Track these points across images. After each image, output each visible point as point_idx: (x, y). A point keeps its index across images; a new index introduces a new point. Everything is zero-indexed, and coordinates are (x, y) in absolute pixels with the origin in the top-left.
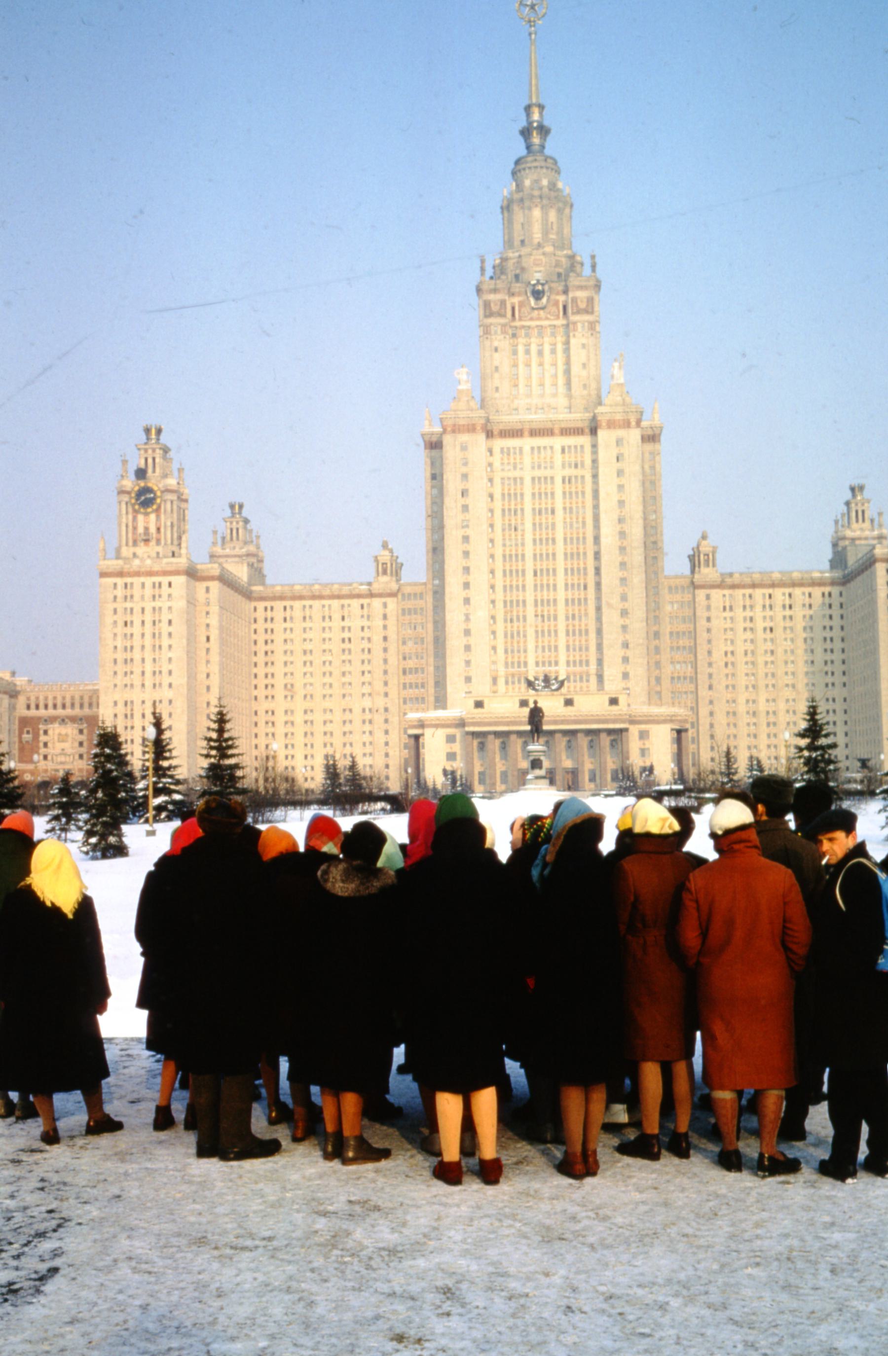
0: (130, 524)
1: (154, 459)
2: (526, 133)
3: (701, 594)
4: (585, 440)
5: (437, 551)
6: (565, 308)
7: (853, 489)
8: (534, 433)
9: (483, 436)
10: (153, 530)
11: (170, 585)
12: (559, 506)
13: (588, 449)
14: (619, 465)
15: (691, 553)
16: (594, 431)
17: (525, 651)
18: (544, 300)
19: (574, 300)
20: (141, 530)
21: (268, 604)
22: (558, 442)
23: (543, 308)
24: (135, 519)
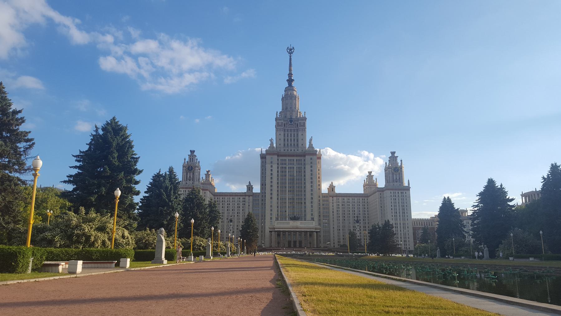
0: (186, 175)
1: (193, 158)
2: (287, 80)
3: (331, 198)
4: (302, 158)
5: (263, 185)
6: (297, 124)
7: (369, 172)
8: (289, 156)
9: (276, 156)
10: (192, 176)
12: (295, 175)
13: (303, 160)
14: (311, 165)
15: (328, 187)
16: (304, 156)
17: (286, 211)
18: (292, 123)
21: (218, 197)
22: (295, 158)
23: (292, 125)
24: (187, 174)
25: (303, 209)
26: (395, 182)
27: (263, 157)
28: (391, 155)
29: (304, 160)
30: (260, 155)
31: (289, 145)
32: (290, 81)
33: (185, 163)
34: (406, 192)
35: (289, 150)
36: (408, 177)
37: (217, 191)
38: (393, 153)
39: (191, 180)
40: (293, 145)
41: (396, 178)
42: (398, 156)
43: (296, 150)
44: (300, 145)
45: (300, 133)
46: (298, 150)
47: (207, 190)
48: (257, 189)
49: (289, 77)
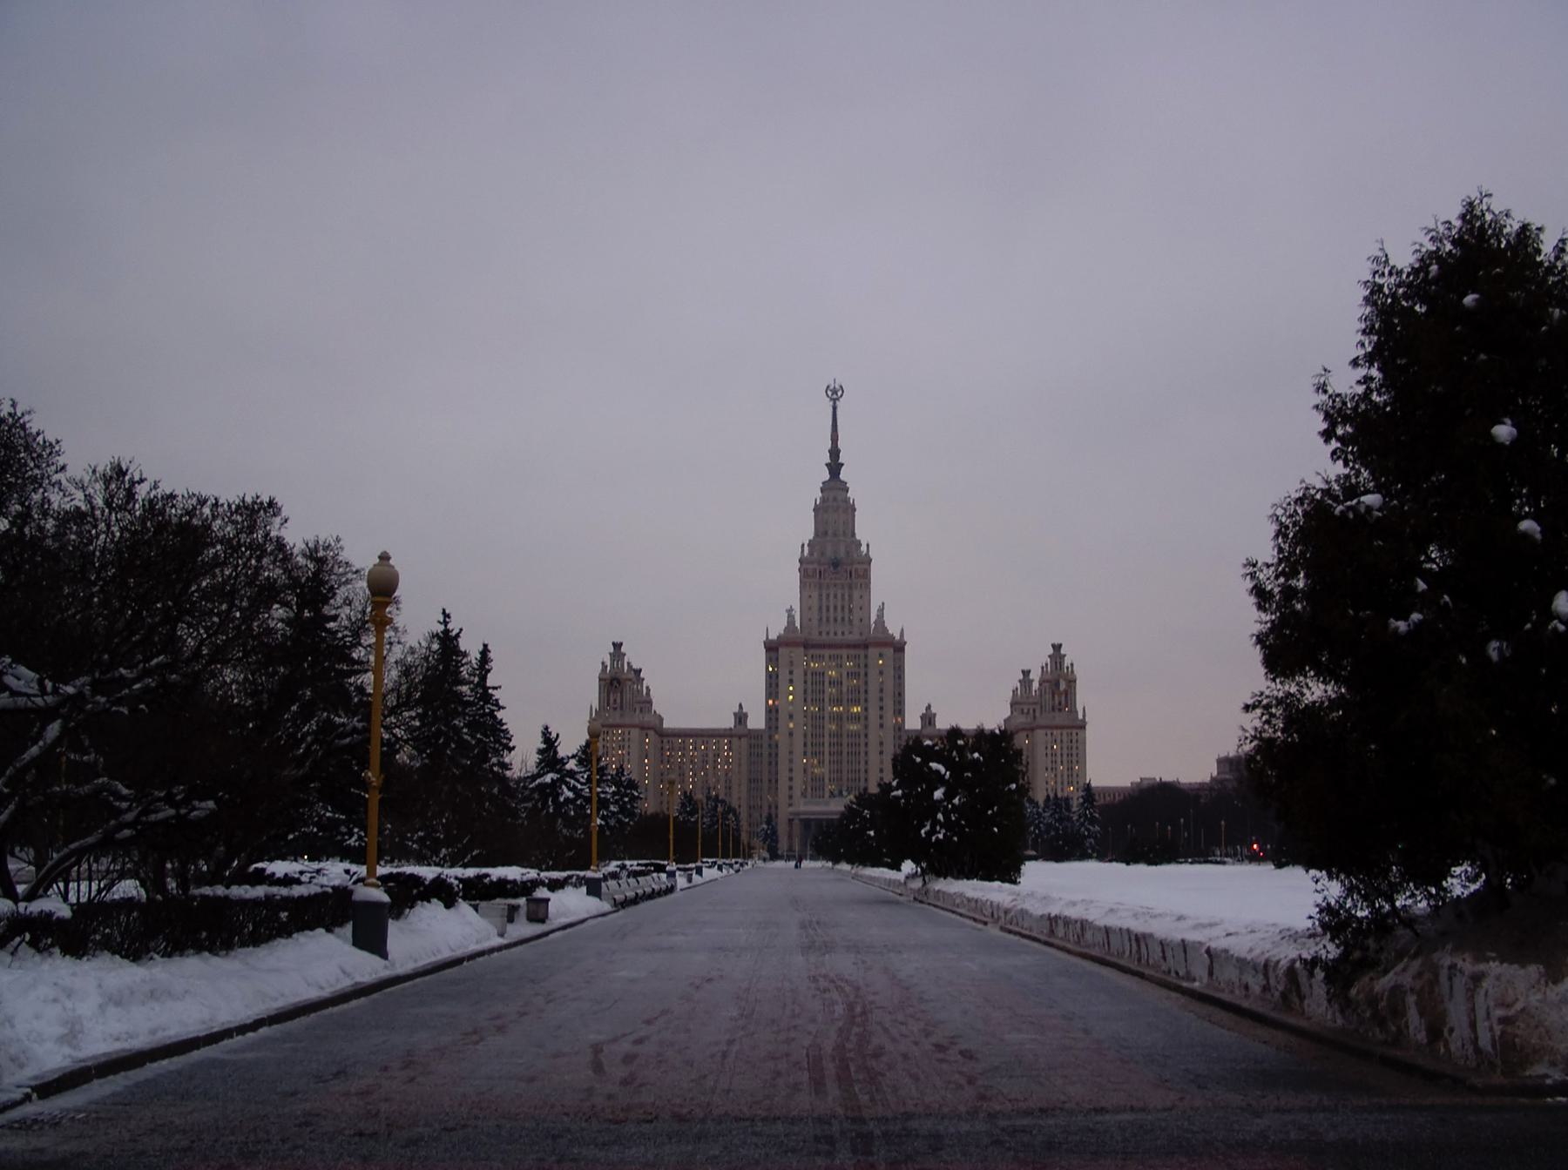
4: (862, 652)
5: (772, 713)
8: (831, 646)
10: (619, 701)
11: (629, 733)
13: (862, 657)
16: (866, 646)
18: (839, 568)
19: (856, 570)
20: (612, 701)
21: (670, 739)
24: (608, 696)
25: (862, 767)
26: (1057, 711)
27: (772, 648)
28: (1051, 651)
29: (866, 657)
30: (765, 643)
31: (832, 619)
32: (835, 467)
33: (602, 670)
34: (1077, 734)
35: (832, 634)
36: (1085, 699)
37: (665, 725)
38: (1057, 647)
39: (618, 709)
40: (839, 619)
41: (1060, 704)
42: (1065, 656)
43: (846, 633)
44: (856, 622)
45: (856, 594)
46: (850, 633)
47: (649, 728)
48: (757, 721)
49: (830, 456)
